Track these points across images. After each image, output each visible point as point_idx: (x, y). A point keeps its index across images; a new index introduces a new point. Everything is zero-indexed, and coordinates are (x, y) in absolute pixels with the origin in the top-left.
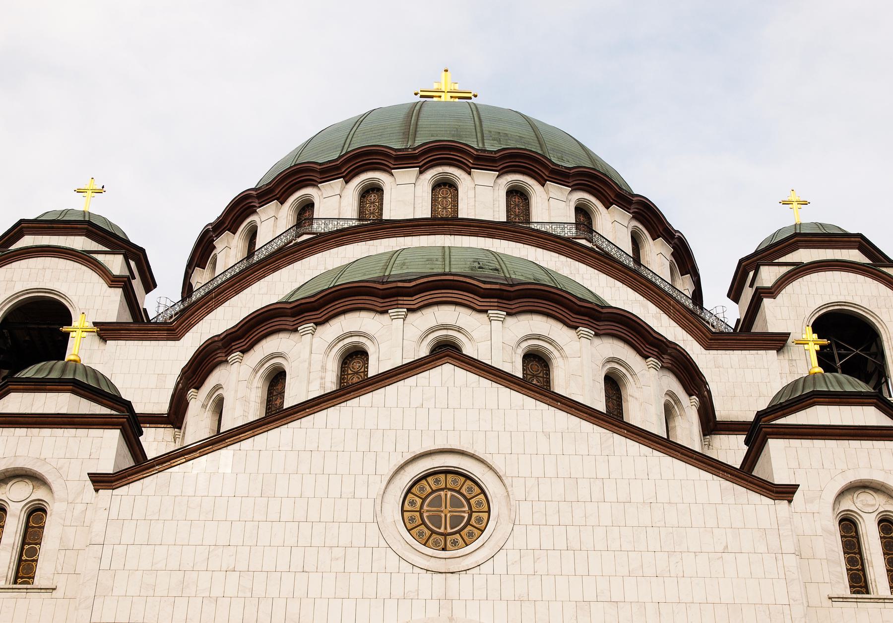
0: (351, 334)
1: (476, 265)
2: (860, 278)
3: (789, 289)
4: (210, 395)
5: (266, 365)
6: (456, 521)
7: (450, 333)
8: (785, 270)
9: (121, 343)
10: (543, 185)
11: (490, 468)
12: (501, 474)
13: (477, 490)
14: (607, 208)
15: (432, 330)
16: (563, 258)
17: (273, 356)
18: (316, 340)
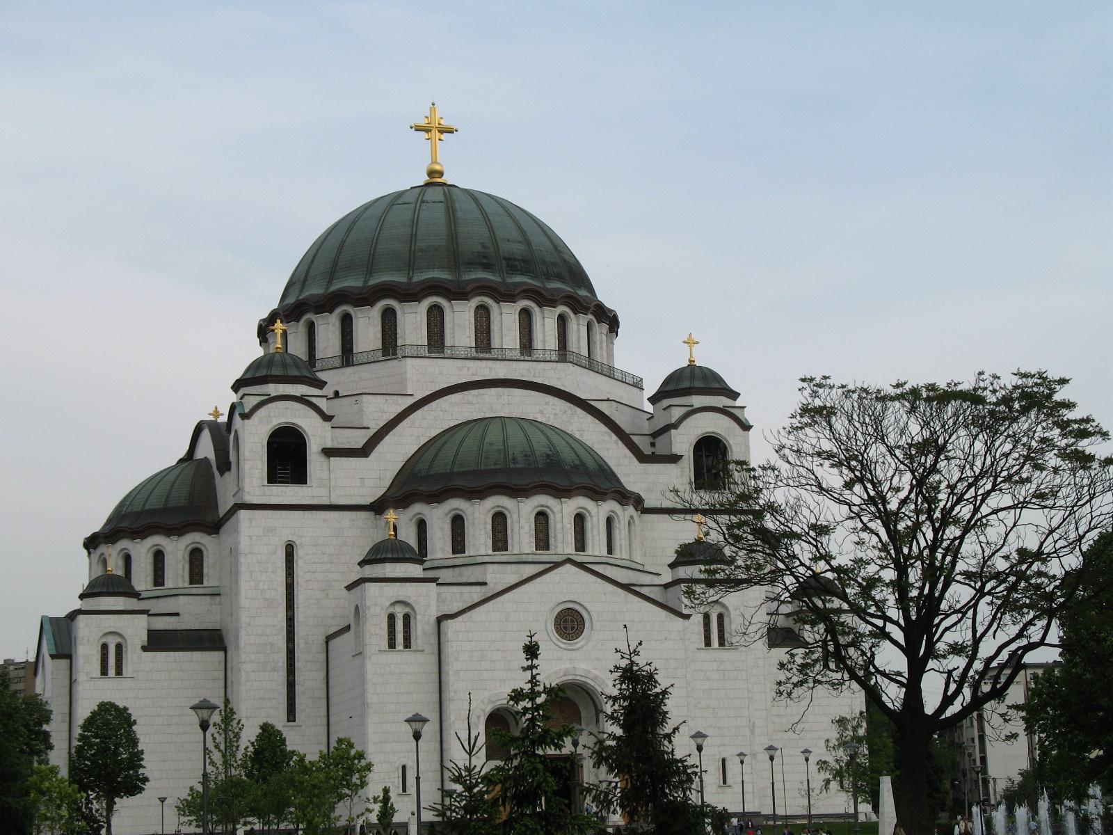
0: (498, 506)
1: (548, 461)
2: (722, 416)
3: (684, 423)
4: (415, 515)
5: (453, 512)
6: (573, 628)
7: (544, 508)
8: (684, 410)
9: (338, 458)
10: (541, 307)
11: (584, 607)
12: (589, 610)
13: (579, 616)
14: (576, 314)
15: (536, 507)
16: (568, 404)
17: (456, 509)
18: (481, 507)
